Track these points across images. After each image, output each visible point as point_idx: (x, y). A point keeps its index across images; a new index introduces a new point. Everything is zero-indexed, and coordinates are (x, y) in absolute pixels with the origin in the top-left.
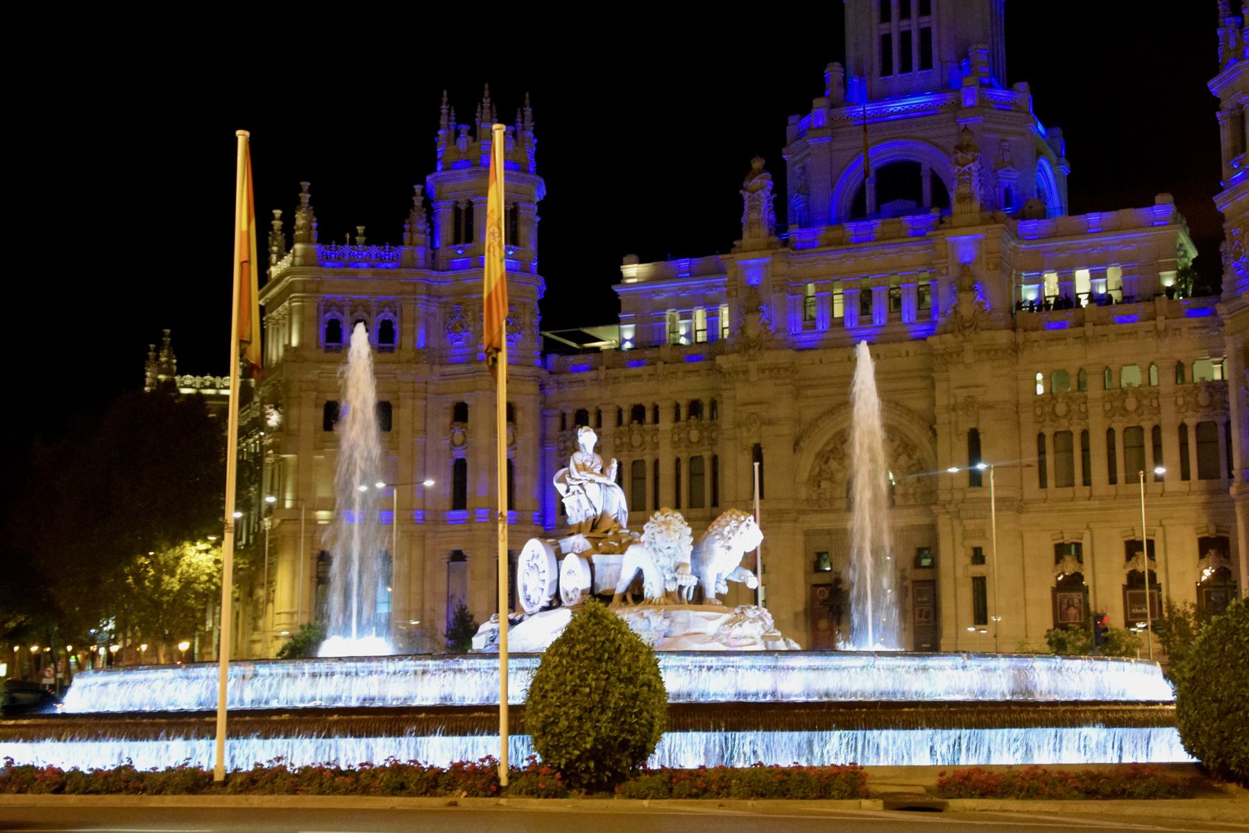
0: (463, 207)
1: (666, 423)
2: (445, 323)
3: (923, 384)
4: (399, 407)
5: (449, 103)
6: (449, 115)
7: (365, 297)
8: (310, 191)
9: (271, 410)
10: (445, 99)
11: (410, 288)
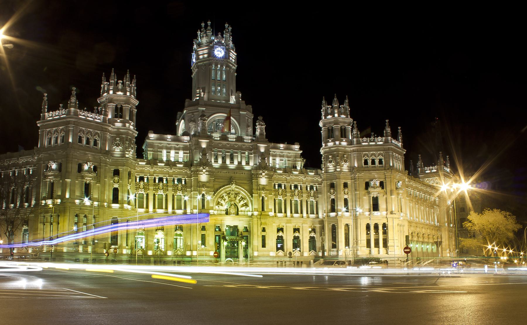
0: (119, 107)
1: (170, 184)
2: (112, 143)
3: (248, 182)
4: (100, 168)
5: (115, 73)
6: (114, 76)
7: (91, 130)
8: (76, 91)
9: (53, 163)
10: (113, 71)
11: (105, 130)
